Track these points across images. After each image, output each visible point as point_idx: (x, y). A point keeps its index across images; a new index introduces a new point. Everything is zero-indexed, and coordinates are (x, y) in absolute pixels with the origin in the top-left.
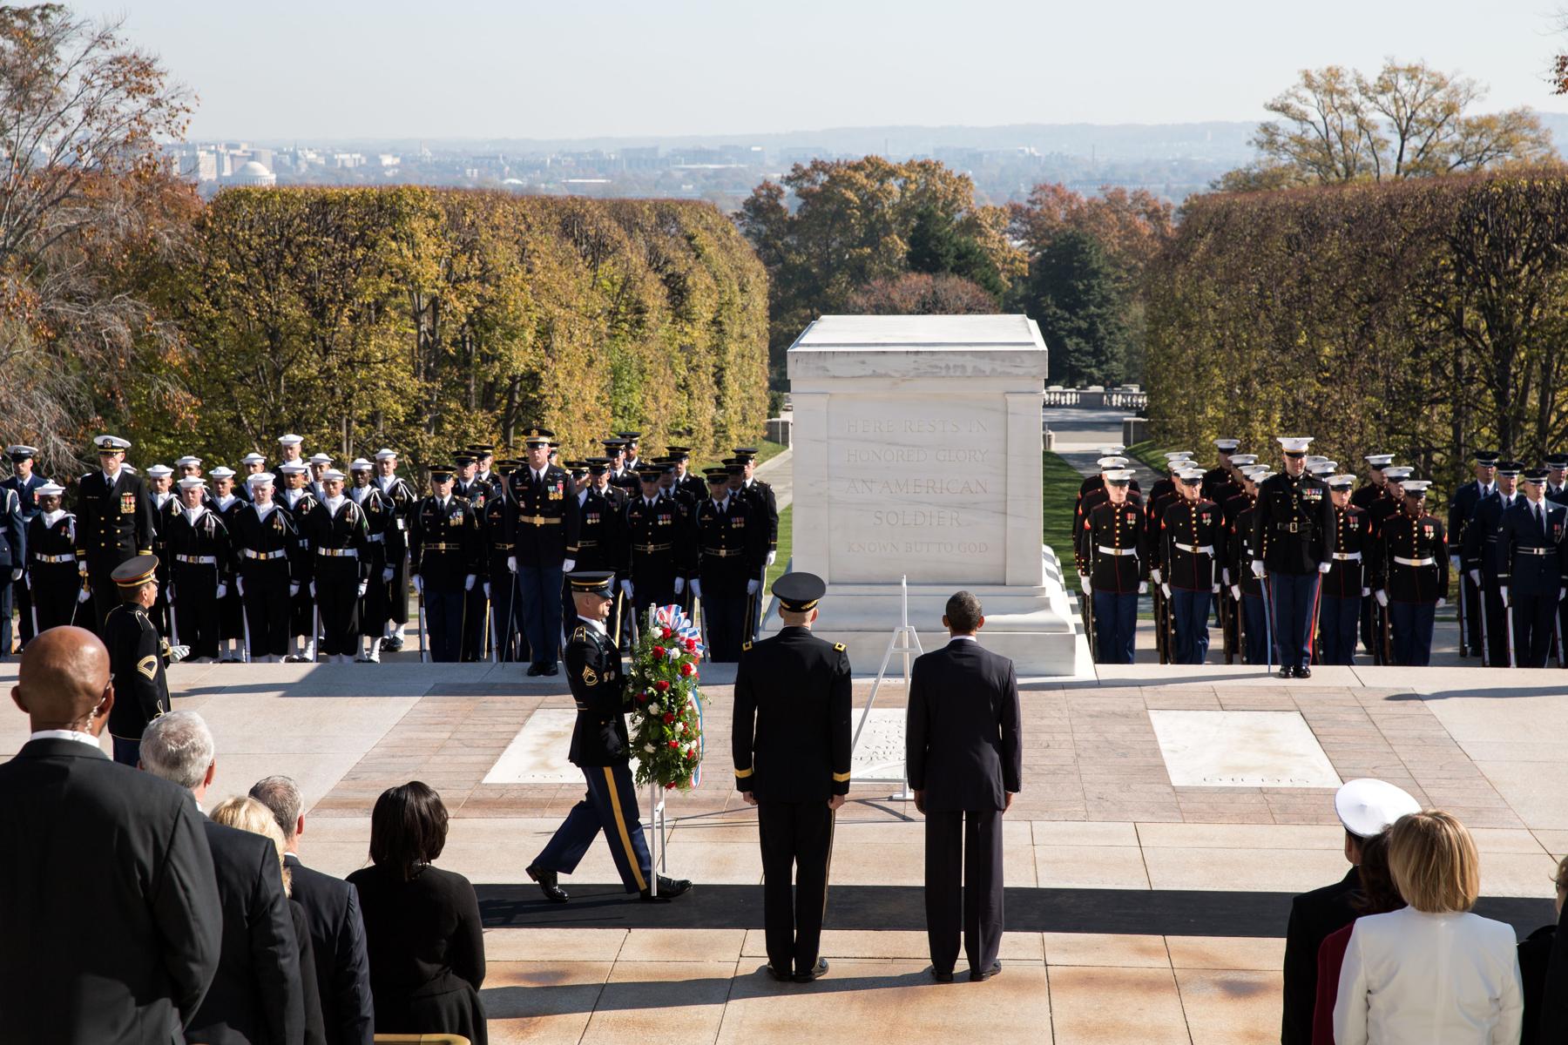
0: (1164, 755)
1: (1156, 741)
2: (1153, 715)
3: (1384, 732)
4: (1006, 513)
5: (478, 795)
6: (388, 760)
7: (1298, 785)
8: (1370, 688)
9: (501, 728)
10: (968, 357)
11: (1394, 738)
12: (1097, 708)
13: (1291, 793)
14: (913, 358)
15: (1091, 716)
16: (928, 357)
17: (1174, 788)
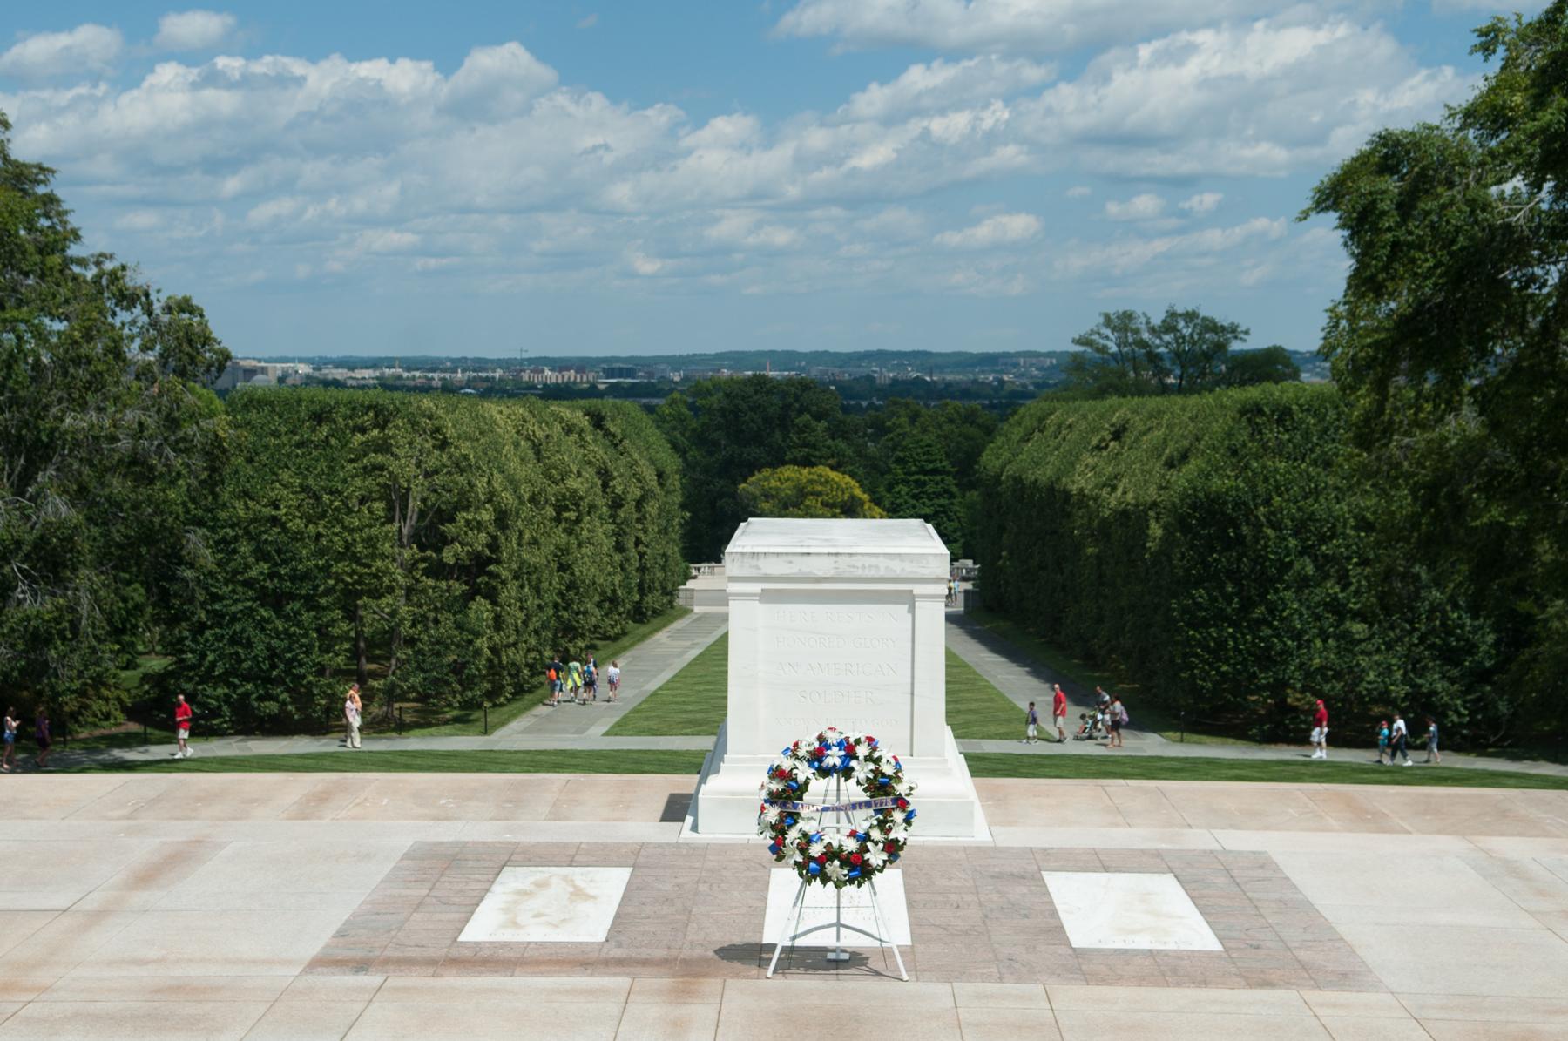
0: (1061, 916)
1: (1052, 902)
2: (1046, 875)
3: (1249, 894)
4: (912, 694)
5: (454, 953)
6: (374, 917)
7: (1183, 947)
8: (1230, 852)
9: (473, 886)
10: (881, 558)
11: (1259, 900)
12: (997, 870)
13: (1179, 955)
14: (833, 558)
15: (992, 877)
16: (847, 559)
17: (1074, 949)
